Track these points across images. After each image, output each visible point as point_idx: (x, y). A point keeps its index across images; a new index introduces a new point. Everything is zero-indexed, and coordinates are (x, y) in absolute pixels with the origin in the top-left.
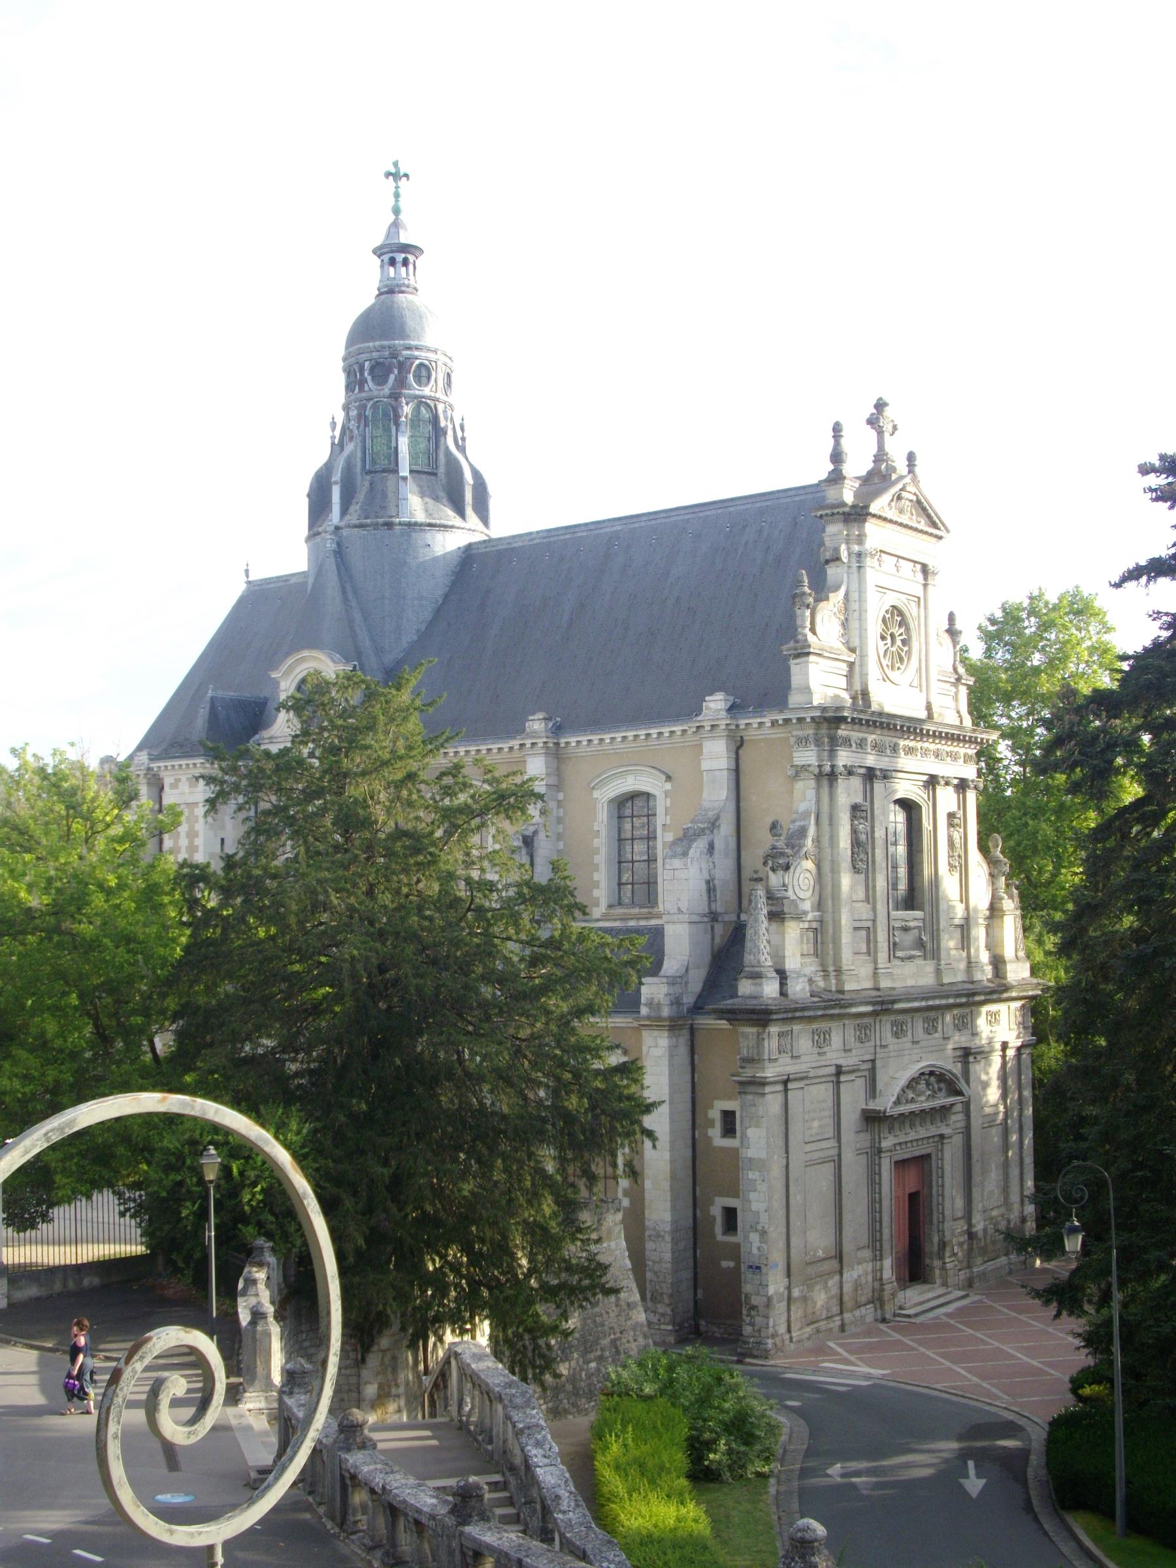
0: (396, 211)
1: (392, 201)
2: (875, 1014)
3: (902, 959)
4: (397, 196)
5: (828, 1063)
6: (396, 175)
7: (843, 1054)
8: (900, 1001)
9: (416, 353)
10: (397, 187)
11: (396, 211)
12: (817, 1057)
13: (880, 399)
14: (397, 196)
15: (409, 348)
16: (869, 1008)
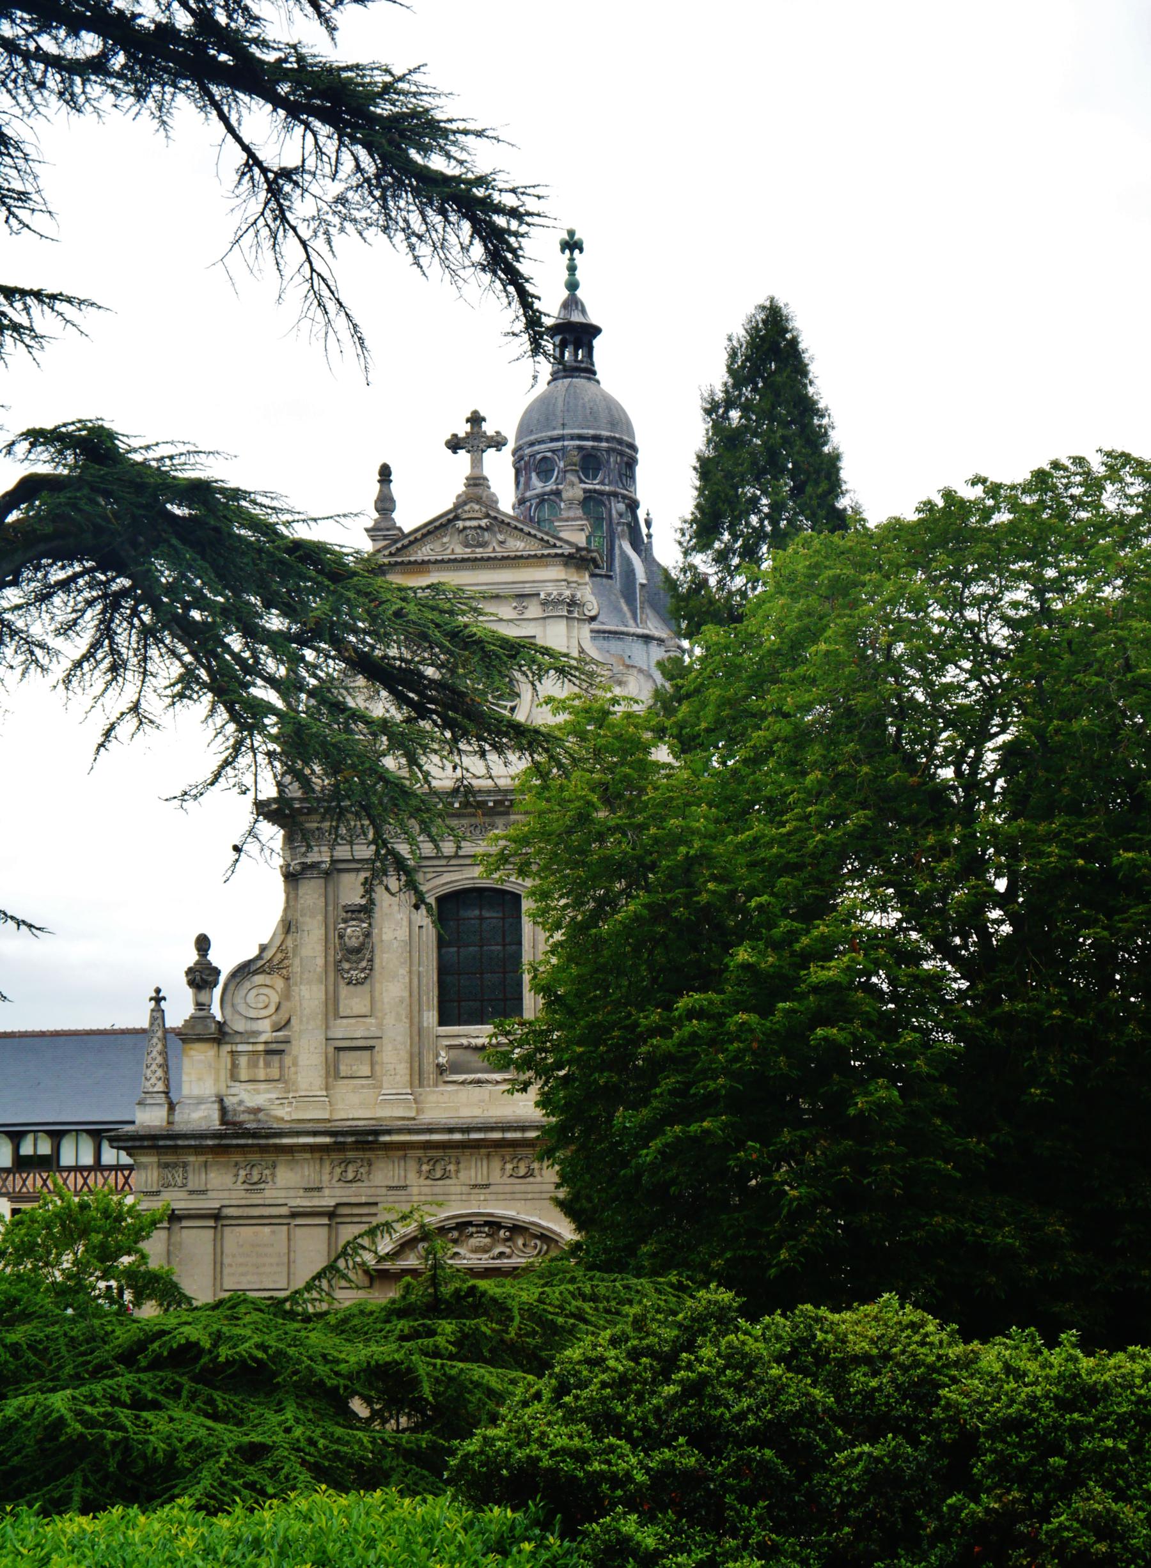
0: (572, 286)
1: (565, 275)
2: (339, 1147)
3: (463, 1083)
4: (572, 269)
5: (268, 1202)
6: (572, 245)
7: (301, 1193)
8: (389, 1132)
9: (536, 448)
10: (572, 259)
11: (572, 286)
12: (243, 1194)
13: (475, 413)
14: (572, 269)
15: (532, 444)
16: (327, 1140)
